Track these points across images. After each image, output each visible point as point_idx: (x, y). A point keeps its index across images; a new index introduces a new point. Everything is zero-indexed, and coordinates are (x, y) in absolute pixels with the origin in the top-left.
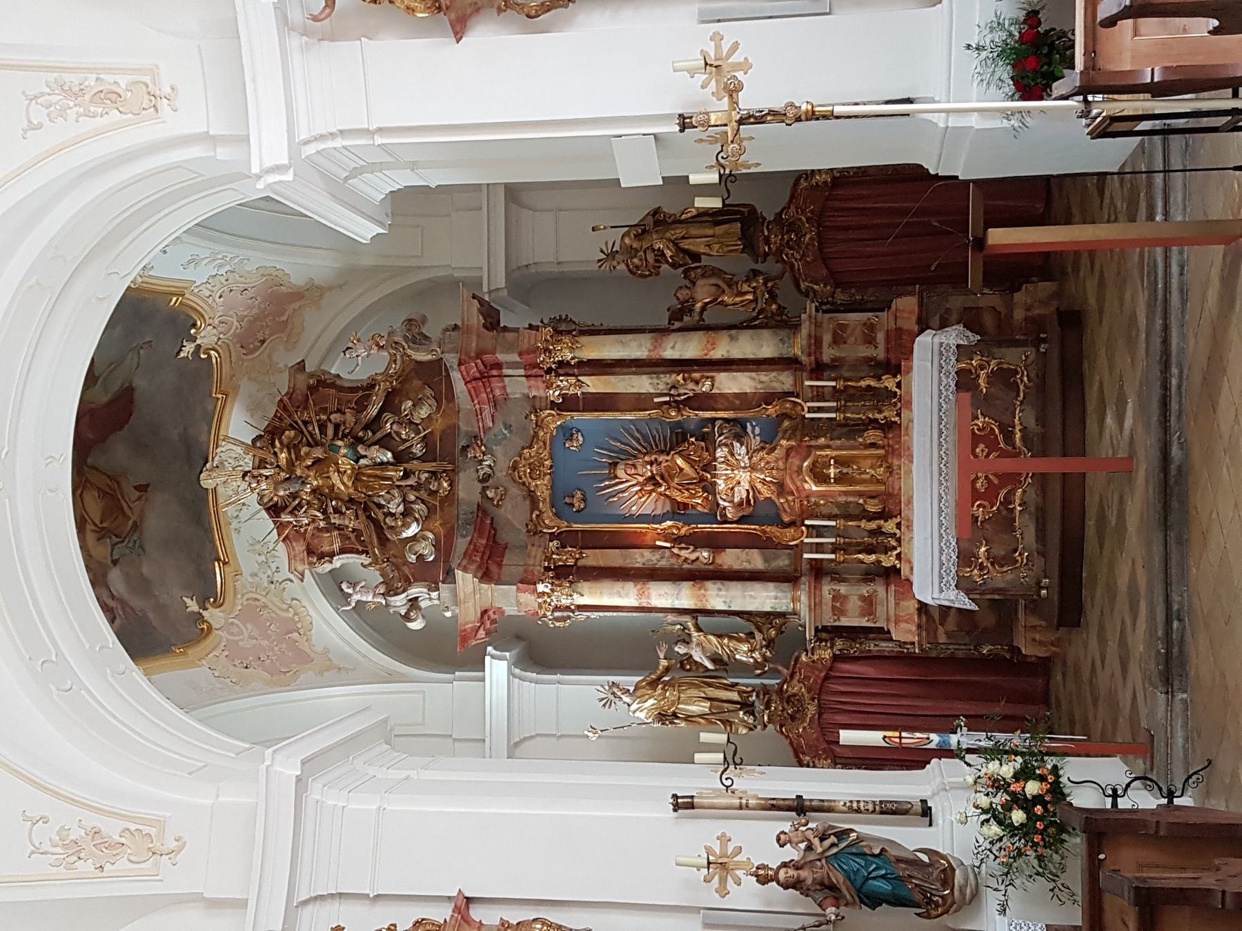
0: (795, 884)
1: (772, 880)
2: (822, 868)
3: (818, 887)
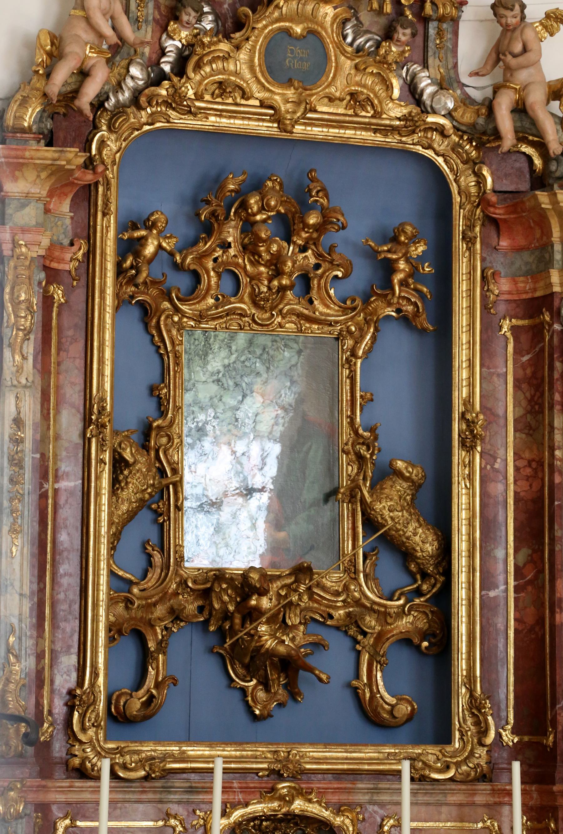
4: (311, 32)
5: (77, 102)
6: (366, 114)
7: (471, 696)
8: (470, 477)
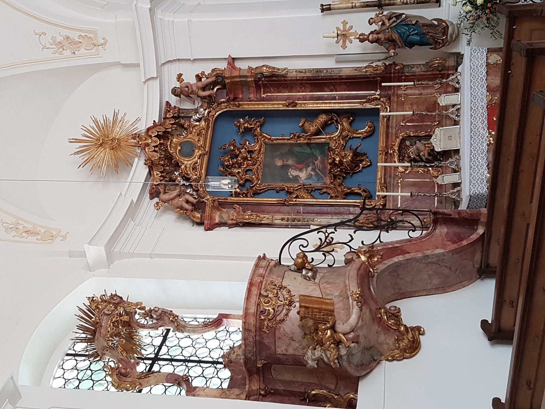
0: (377, 41)
1: (366, 40)
2: (389, 32)
3: (387, 41)
4: (180, 145)
5: (195, 203)
6: (204, 132)
7: (366, 102)
8: (304, 104)
